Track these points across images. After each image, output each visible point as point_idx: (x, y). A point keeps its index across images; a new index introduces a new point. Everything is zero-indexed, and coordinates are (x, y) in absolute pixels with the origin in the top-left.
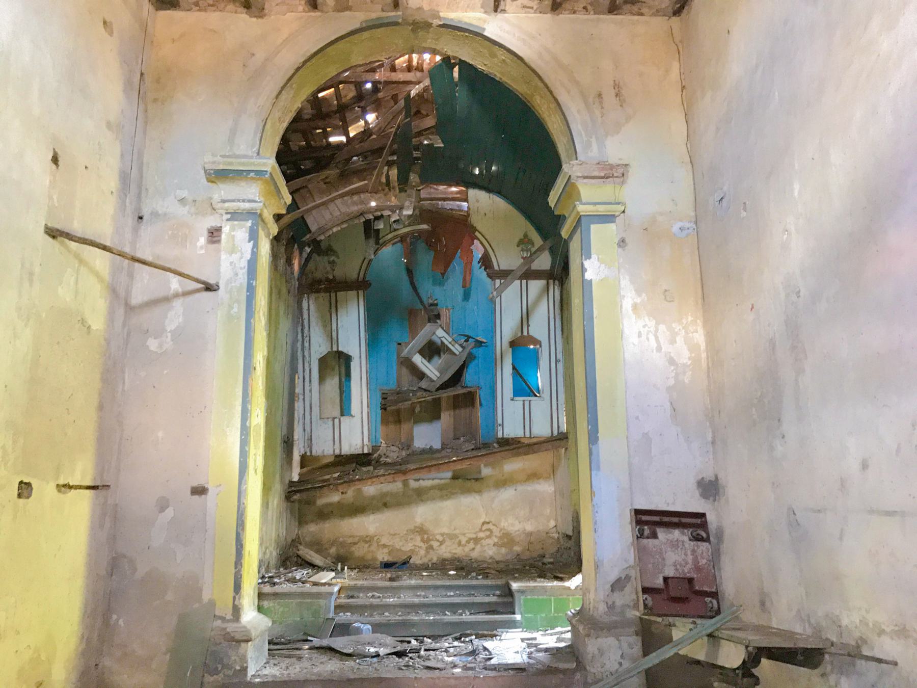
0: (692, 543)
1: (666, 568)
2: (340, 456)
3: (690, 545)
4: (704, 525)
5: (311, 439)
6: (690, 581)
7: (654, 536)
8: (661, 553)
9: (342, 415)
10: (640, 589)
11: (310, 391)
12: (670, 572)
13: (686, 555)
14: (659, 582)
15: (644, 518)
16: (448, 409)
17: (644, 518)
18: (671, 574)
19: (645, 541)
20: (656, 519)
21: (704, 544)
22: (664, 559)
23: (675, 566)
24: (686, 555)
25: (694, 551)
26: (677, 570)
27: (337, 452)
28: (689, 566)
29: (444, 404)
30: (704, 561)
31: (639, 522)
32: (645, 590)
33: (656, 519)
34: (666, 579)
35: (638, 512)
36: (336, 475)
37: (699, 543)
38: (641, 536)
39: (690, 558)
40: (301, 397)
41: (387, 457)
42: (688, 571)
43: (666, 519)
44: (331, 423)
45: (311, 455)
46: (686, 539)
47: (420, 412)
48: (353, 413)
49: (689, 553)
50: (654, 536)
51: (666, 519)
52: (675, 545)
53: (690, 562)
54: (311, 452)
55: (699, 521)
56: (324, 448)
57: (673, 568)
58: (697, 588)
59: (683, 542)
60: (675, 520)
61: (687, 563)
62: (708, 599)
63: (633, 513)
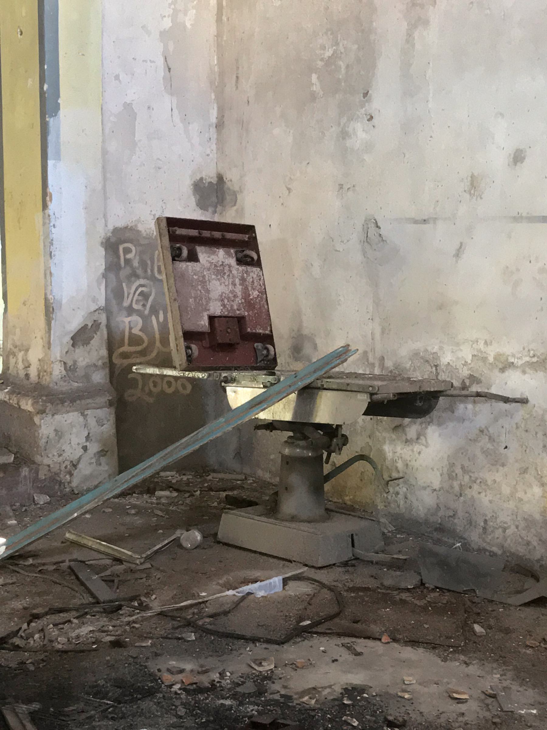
0: (241, 268)
1: (211, 304)
3: (237, 270)
4: (253, 243)
6: (240, 320)
7: (193, 257)
8: (203, 282)
10: (181, 334)
12: (216, 309)
13: (234, 285)
14: (204, 323)
15: (181, 231)
17: (181, 231)
18: (218, 313)
19: (183, 266)
20: (193, 233)
21: (254, 269)
22: (208, 291)
23: (222, 300)
24: (234, 285)
25: (243, 280)
26: (224, 306)
28: (239, 300)
30: (256, 293)
31: (173, 238)
32: (189, 336)
33: (193, 233)
34: (212, 318)
35: (172, 222)
37: (249, 268)
38: (176, 256)
39: (239, 289)
42: (236, 307)
43: (206, 234)
46: (232, 261)
49: (237, 281)
50: (193, 257)
51: (206, 234)
52: (220, 271)
53: (239, 294)
55: (246, 237)
57: (219, 304)
58: (249, 330)
59: (230, 266)
60: (217, 235)
61: (235, 296)
62: (258, 345)
63: (164, 224)
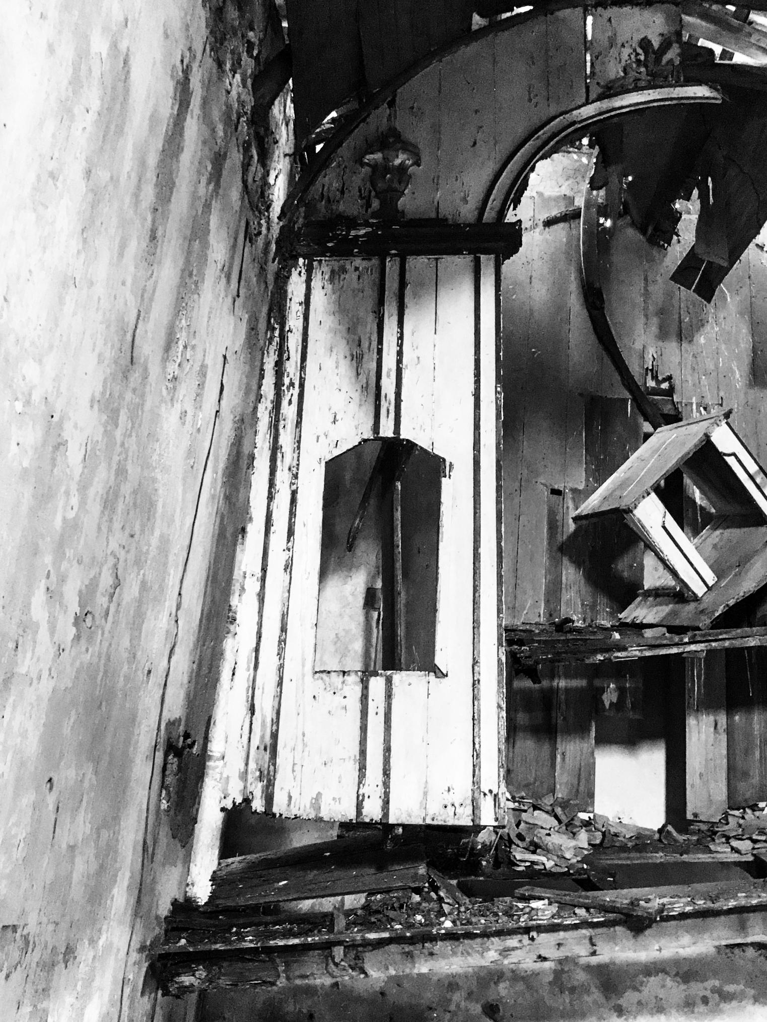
2: (385, 827)
5: (273, 749)
9: (392, 662)
11: (288, 567)
16: (708, 705)
27: (372, 811)
29: (696, 687)
36: (354, 901)
40: (252, 586)
41: (534, 847)
44: (358, 689)
45: (269, 812)
47: (618, 706)
48: (440, 660)
54: (269, 799)
56: (319, 789)
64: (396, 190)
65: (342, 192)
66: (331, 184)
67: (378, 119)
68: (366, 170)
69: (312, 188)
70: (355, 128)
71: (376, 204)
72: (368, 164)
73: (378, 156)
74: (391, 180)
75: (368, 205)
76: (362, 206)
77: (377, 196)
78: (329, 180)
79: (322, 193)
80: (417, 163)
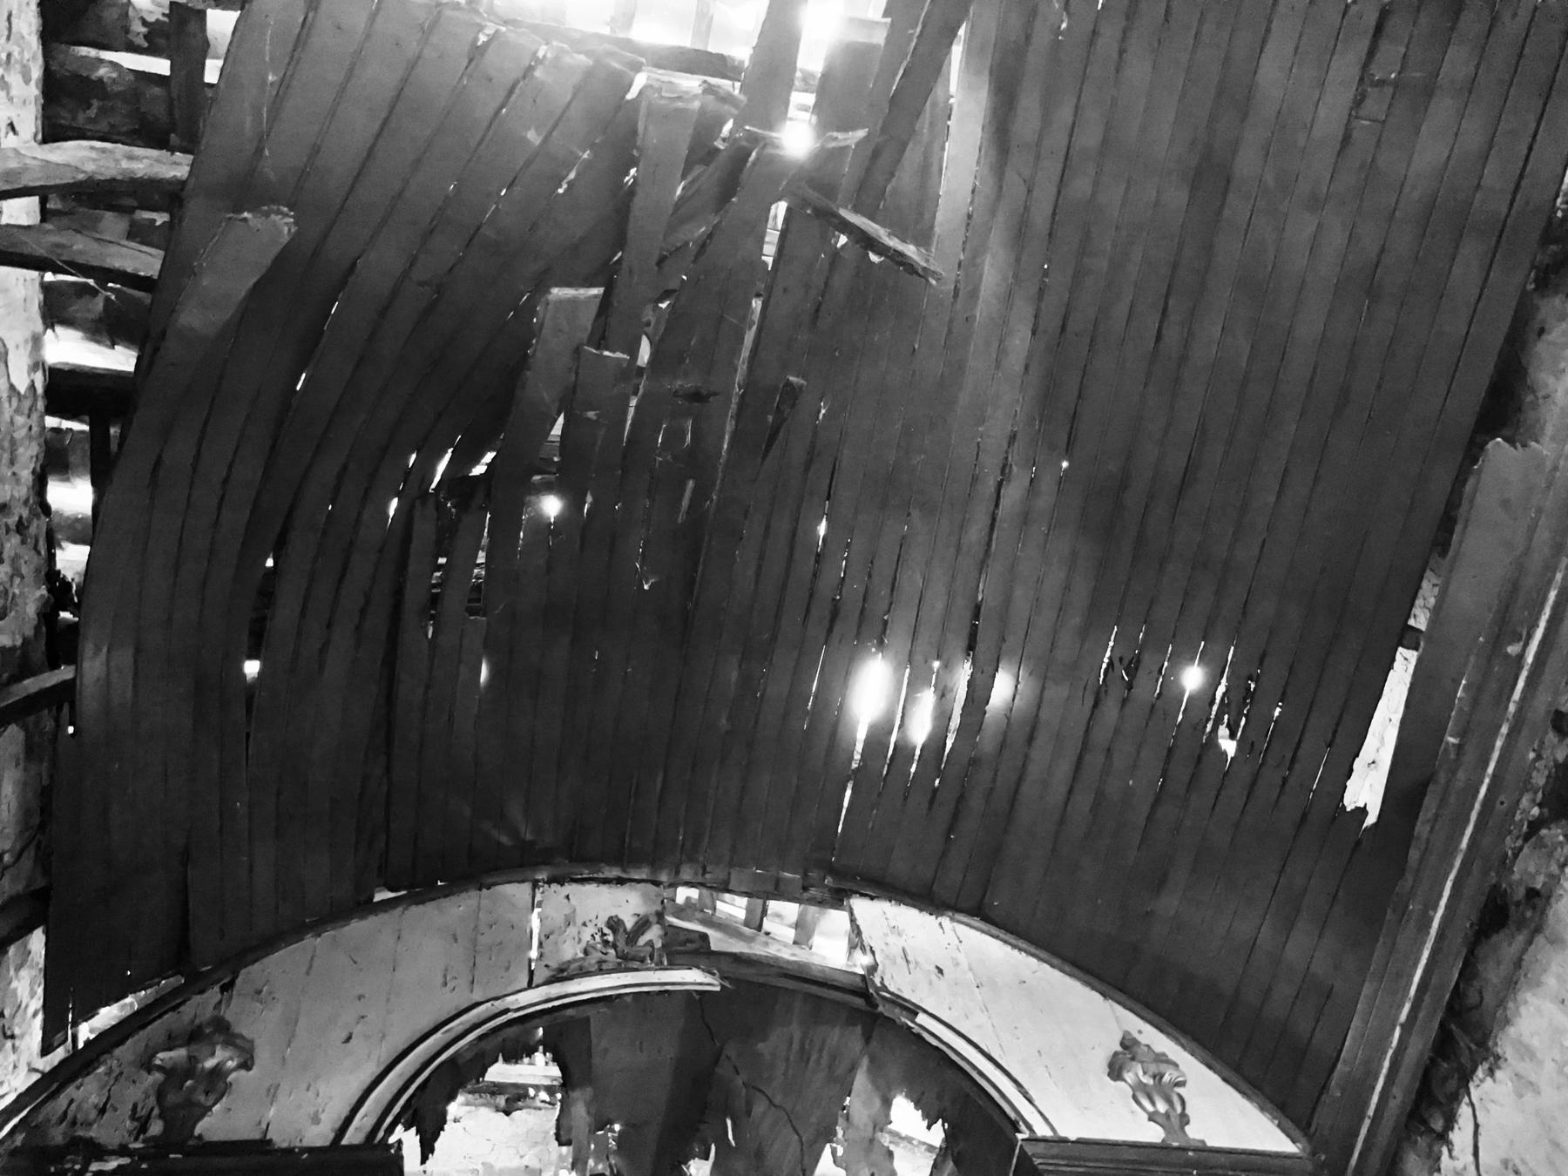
64: (199, 1105)
65: (102, 1111)
66: (85, 1099)
67: (201, 1006)
68: (158, 1076)
69: (49, 1107)
70: (154, 1020)
71: (156, 1128)
72: (160, 1068)
73: (180, 1053)
74: (192, 1089)
75: (143, 1128)
76: (130, 1133)
77: (161, 1116)
78: (87, 1092)
79: (65, 1112)
80: (246, 1065)
